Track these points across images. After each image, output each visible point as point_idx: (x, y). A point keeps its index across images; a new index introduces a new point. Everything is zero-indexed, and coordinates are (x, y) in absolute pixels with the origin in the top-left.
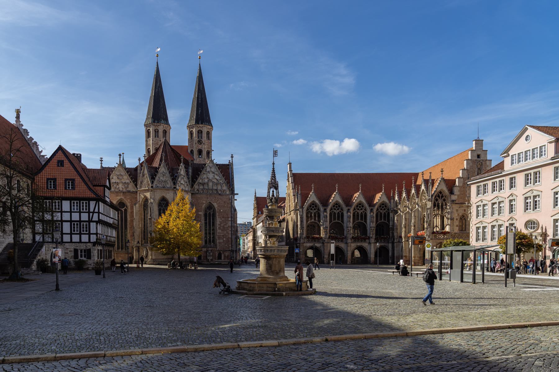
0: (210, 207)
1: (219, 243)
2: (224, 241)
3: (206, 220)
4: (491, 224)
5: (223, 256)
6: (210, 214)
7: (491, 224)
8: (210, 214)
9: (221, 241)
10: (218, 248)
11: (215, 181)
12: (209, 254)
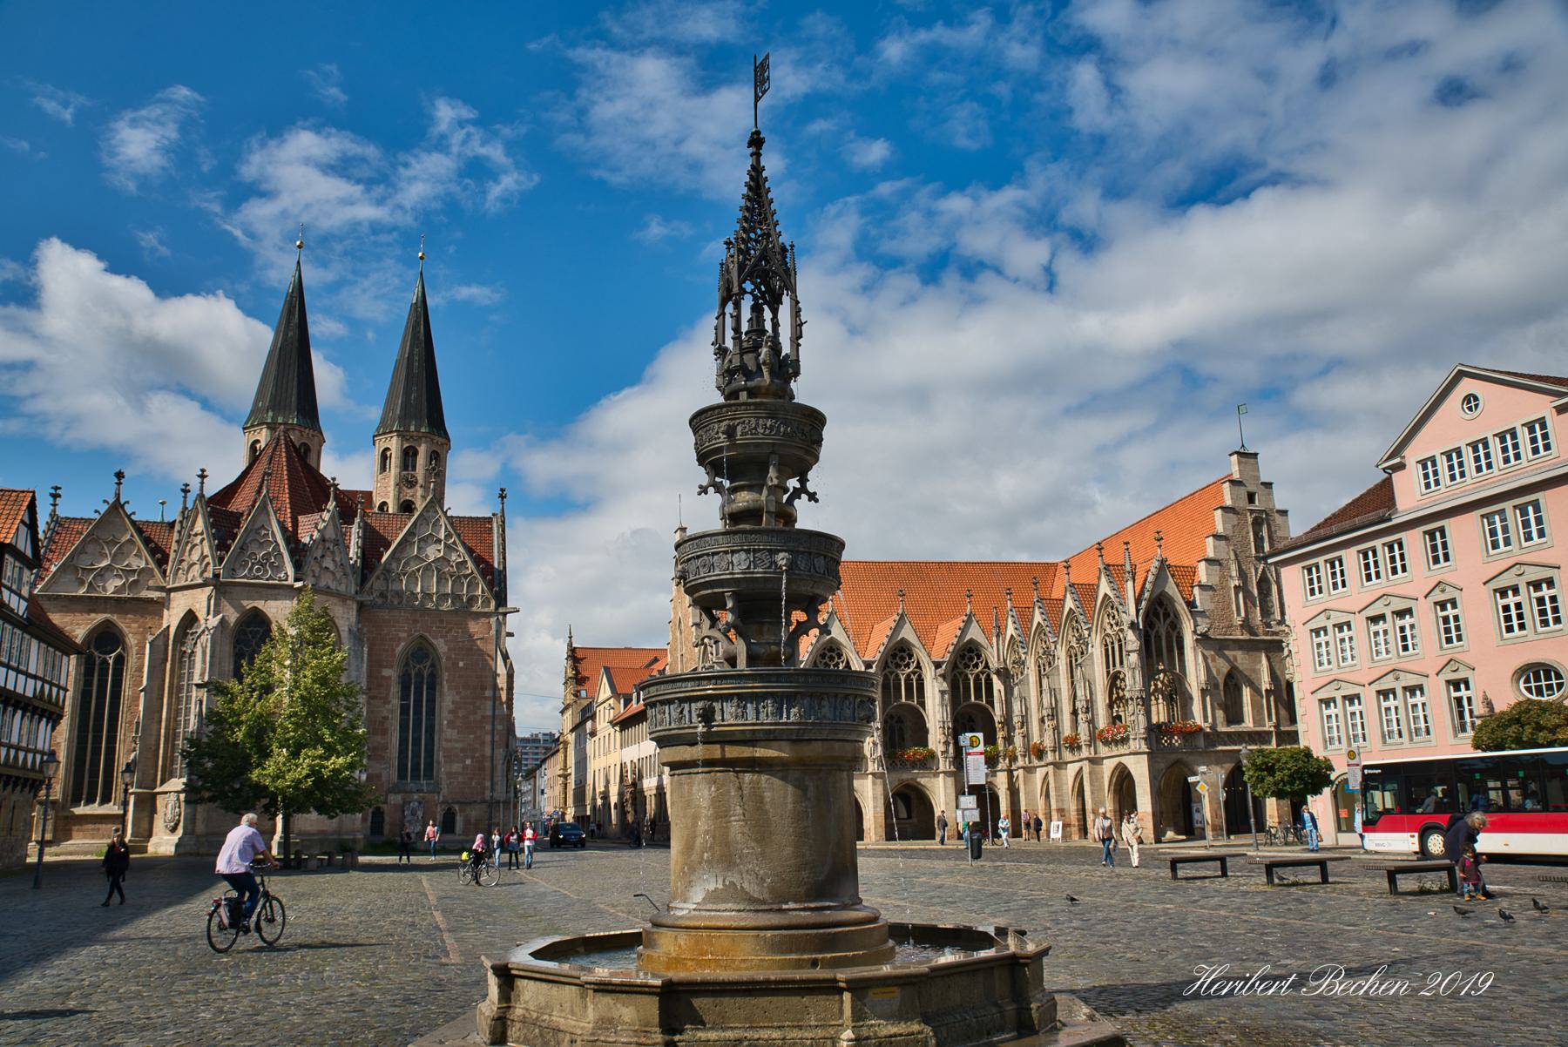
0: (421, 652)
1: (450, 774)
2: (465, 767)
3: (405, 696)
4: (1376, 687)
5: (459, 819)
6: (419, 674)
7: (1376, 687)
8: (419, 674)
9: (457, 767)
10: (445, 791)
12: (414, 813)
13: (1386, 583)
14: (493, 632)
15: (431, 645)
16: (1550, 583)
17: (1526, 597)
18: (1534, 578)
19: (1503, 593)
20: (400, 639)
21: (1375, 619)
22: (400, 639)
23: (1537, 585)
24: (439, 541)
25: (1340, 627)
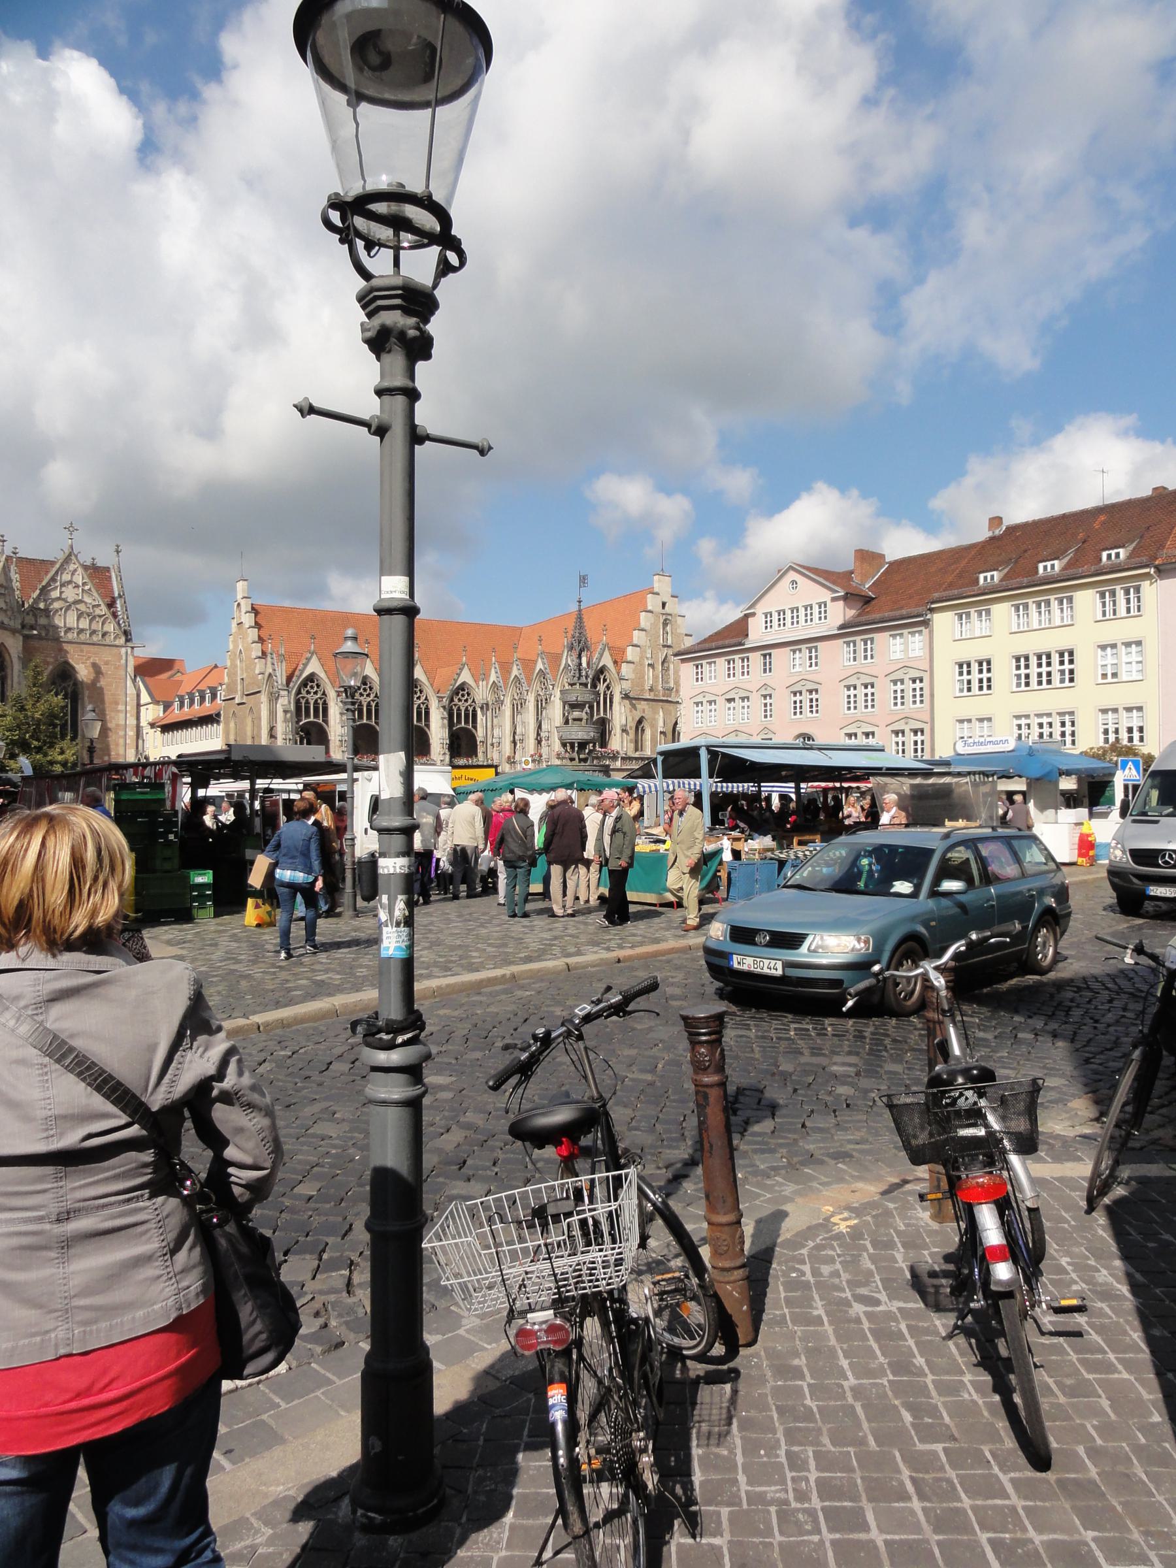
11: (82, 607)
13: (738, 680)
14: (123, 662)
15: (73, 668)
16: (817, 691)
17: (806, 697)
18: (810, 688)
19: (795, 694)
20: (48, 663)
21: (729, 700)
22: (48, 663)
23: (811, 692)
24: (77, 586)
25: (710, 702)
